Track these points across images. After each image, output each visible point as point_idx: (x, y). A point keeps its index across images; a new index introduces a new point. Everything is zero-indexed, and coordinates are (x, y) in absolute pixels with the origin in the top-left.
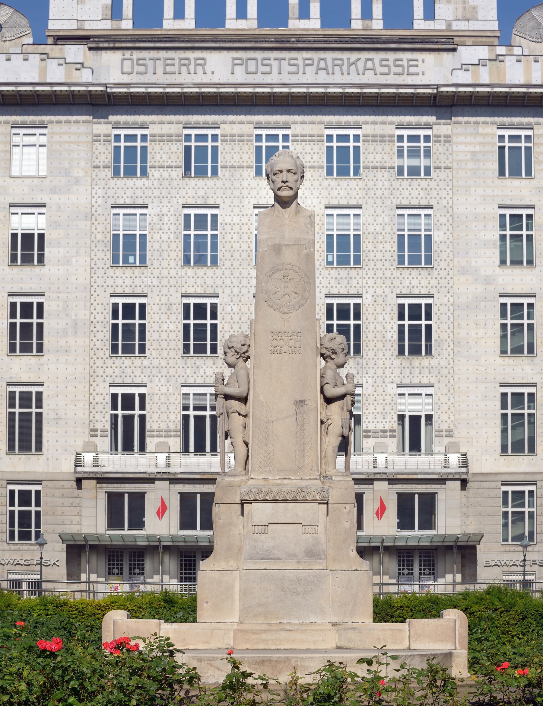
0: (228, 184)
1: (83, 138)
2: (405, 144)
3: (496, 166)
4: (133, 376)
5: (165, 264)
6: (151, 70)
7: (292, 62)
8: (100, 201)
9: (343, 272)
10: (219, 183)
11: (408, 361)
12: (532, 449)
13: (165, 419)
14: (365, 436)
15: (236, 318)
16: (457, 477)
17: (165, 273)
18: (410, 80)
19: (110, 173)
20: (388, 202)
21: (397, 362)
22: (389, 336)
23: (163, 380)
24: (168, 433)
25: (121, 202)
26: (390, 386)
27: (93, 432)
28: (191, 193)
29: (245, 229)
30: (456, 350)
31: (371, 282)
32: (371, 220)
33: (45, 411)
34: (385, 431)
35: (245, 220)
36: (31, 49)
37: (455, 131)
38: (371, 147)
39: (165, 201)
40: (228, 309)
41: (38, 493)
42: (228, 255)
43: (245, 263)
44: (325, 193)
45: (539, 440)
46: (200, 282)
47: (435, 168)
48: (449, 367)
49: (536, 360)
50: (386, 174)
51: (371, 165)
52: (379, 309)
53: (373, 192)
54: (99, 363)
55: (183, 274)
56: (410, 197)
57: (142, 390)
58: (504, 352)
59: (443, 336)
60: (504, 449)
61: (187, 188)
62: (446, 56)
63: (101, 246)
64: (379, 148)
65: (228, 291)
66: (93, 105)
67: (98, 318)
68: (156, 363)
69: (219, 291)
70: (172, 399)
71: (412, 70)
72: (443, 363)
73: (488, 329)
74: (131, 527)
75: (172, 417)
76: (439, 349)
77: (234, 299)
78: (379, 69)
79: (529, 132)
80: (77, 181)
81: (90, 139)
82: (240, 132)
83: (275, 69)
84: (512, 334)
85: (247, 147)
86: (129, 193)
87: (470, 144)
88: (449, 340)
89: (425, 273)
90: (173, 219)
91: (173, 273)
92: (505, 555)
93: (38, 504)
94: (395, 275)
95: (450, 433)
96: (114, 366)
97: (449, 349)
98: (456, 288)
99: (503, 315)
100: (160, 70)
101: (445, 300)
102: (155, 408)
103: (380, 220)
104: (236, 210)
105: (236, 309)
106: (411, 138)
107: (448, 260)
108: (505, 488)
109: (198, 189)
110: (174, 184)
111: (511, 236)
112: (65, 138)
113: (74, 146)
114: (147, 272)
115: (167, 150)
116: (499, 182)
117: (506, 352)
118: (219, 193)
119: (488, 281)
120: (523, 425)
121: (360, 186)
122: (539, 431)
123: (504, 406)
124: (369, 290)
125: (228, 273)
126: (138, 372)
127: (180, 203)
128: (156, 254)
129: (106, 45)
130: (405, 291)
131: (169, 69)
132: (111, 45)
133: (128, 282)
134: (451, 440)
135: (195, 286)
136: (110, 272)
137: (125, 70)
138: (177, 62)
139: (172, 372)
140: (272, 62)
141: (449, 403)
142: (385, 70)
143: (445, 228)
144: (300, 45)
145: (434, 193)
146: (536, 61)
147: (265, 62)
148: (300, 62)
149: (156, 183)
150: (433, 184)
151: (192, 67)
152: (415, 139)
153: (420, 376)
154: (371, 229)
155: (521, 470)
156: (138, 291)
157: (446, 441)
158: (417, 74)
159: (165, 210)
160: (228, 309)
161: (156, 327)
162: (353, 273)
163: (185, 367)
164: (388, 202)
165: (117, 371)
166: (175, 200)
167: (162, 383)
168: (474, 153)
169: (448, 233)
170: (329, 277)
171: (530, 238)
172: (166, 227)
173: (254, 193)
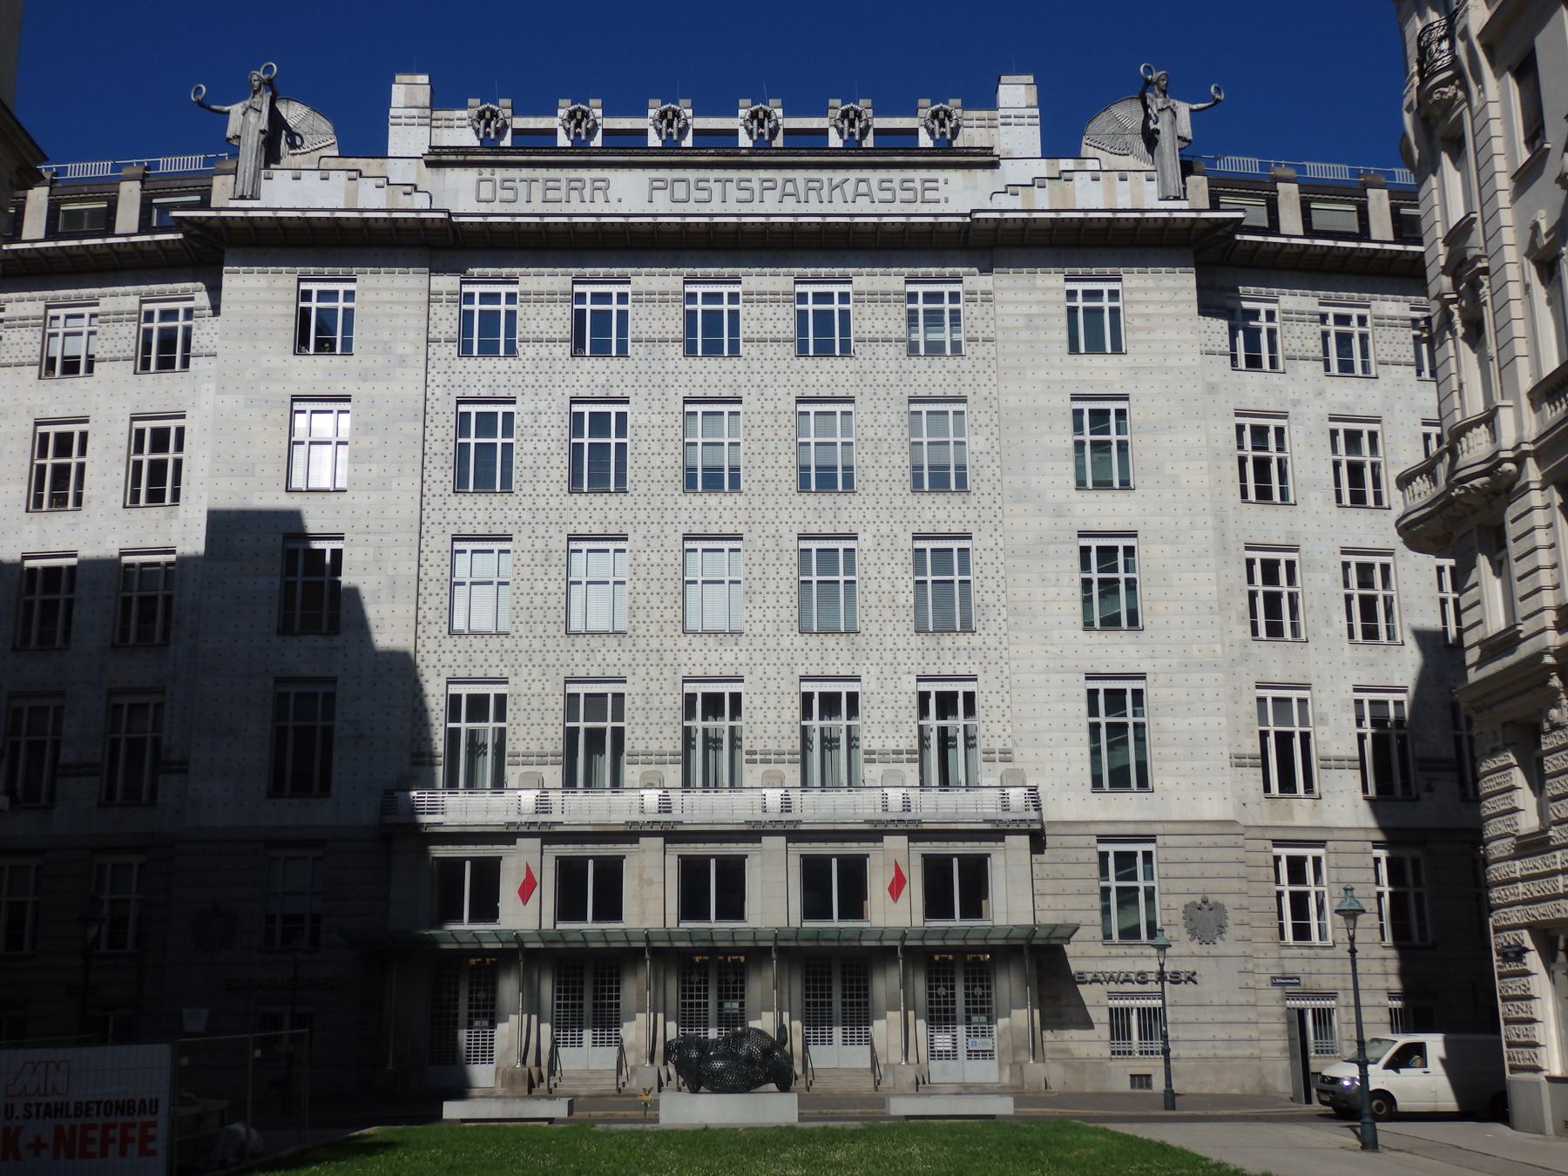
0: (643, 366)
1: (414, 297)
2: (921, 306)
3: (1064, 336)
4: (486, 665)
5: (541, 488)
6: (523, 196)
7: (743, 184)
10: (628, 364)
11: (934, 640)
12: (1143, 782)
13: (538, 734)
14: (867, 761)
15: (655, 572)
16: (1023, 826)
17: (541, 502)
18: (926, 209)
19: (453, 349)
20: (895, 393)
21: (916, 640)
22: (901, 599)
23: (536, 673)
24: (542, 758)
26: (906, 678)
28: (585, 380)
29: (670, 433)
30: (1011, 620)
31: (870, 515)
32: (868, 419)
34: (899, 752)
35: (669, 420)
36: (333, 163)
37: (998, 283)
38: (867, 310)
39: (543, 392)
42: (642, 475)
43: (669, 489)
44: (795, 379)
45: (1153, 767)
46: (597, 516)
47: (969, 340)
48: (1001, 647)
50: (892, 350)
51: (868, 336)
52: (885, 557)
53: (870, 377)
55: (571, 504)
56: (930, 384)
57: (500, 689)
58: (1088, 625)
59: (990, 599)
60: (1097, 782)
61: (578, 372)
62: (981, 175)
64: (879, 310)
65: (642, 530)
68: (524, 644)
69: (627, 530)
70: (550, 702)
71: (929, 195)
72: (991, 642)
73: (1061, 588)
74: (474, 918)
76: (983, 619)
77: (653, 542)
78: (878, 195)
80: (403, 361)
82: (662, 289)
83: (717, 196)
84: (1101, 595)
85: (673, 311)
86: (486, 379)
87: (1023, 302)
88: (999, 605)
89: (956, 499)
90: (555, 420)
91: (554, 502)
92: (1110, 962)
94: (909, 503)
95: (1006, 755)
96: (455, 651)
97: (1000, 619)
98: (1007, 522)
99: (1085, 566)
100: (537, 196)
101: (991, 543)
103: (883, 419)
104: (656, 405)
105: (655, 558)
106: (929, 297)
107: (994, 480)
109: (595, 375)
110: (558, 366)
111: (1093, 443)
113: (398, 309)
115: (547, 314)
117: (1092, 624)
118: (629, 379)
119: (1059, 512)
120: (1125, 742)
121: (851, 368)
123: (1093, 711)
124: (868, 527)
125: (642, 502)
126: (494, 659)
127: (568, 395)
128: (528, 474)
129: (452, 158)
130: (926, 529)
131: (551, 195)
132: (461, 158)
133: (482, 516)
134: (1009, 765)
135: (590, 522)
137: (482, 196)
138: (563, 184)
139: (551, 658)
140: (712, 184)
141: (1003, 706)
142: (888, 195)
143: (987, 431)
144: (754, 159)
145: (967, 379)
146: (1123, 179)
147: (701, 185)
148: (755, 185)
149: (529, 366)
150: (965, 364)
151: (587, 193)
152: (937, 297)
153: (954, 663)
154: (870, 433)
156: (498, 530)
157: (1001, 767)
158: (938, 202)
159: (542, 406)
160: (643, 558)
162: (842, 500)
163: (573, 650)
164: (895, 393)
165: (461, 658)
166: (559, 391)
167: (534, 675)
168: (1030, 317)
169: (992, 438)
170: (805, 508)
171: (1123, 446)
173: (684, 379)
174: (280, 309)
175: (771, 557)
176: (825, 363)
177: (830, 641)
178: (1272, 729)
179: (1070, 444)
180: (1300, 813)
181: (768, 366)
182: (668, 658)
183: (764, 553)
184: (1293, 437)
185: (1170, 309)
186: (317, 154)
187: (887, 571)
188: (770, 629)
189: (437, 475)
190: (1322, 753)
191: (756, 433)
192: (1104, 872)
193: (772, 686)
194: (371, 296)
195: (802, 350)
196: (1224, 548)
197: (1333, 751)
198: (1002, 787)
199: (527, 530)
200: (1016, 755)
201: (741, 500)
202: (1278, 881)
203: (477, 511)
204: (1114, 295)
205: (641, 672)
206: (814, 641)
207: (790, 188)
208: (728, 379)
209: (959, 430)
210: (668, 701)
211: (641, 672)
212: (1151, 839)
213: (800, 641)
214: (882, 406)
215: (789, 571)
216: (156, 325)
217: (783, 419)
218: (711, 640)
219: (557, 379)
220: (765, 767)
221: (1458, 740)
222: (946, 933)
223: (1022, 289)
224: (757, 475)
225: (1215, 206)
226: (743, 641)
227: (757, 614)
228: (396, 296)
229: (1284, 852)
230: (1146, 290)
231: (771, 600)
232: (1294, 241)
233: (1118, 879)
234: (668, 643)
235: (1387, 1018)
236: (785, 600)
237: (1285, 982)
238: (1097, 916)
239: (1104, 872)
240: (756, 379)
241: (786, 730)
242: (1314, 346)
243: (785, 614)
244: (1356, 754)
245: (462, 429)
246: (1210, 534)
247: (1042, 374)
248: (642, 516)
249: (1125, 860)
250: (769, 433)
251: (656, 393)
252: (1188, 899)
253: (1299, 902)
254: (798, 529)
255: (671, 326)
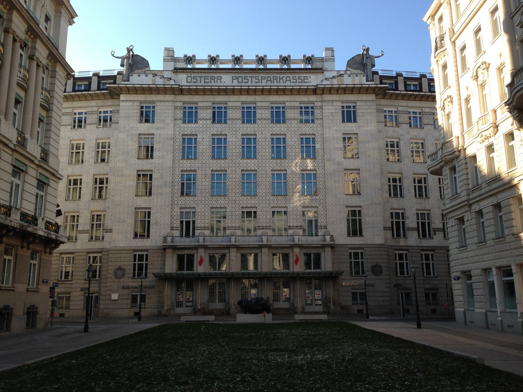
0: (231, 126)
1: (170, 108)
2: (303, 110)
3: (341, 118)
5: (204, 158)
6: (199, 81)
8: (177, 133)
9: (279, 161)
10: (227, 126)
12: (361, 234)
17: (204, 162)
18: (305, 84)
19: (181, 122)
20: (297, 133)
23: (203, 206)
24: (205, 228)
25: (186, 133)
27: (172, 228)
28: (215, 130)
29: (238, 144)
30: (327, 192)
32: (289, 140)
33: (152, 219)
35: (237, 140)
38: (289, 111)
39: (205, 133)
40: (231, 176)
41: (147, 255)
42: (230, 154)
43: (238, 158)
44: (270, 129)
46: (219, 165)
49: (361, 196)
54: (176, 199)
60: (349, 235)
63: (177, 151)
64: (293, 111)
65: (230, 169)
66: (175, 94)
67: (176, 180)
68: (200, 199)
69: (227, 169)
71: (306, 81)
72: (321, 198)
74: (187, 270)
75: (207, 221)
78: (292, 81)
79: (354, 105)
80: (168, 124)
81: (173, 108)
83: (250, 81)
86: (190, 129)
87: (330, 109)
90: (208, 140)
91: (207, 162)
93: (147, 260)
95: (325, 227)
98: (326, 167)
100: (203, 81)
101: (321, 172)
102: (199, 218)
103: (293, 140)
104: (234, 136)
105: (234, 176)
106: (305, 108)
108: (350, 251)
109: (218, 128)
110: (208, 126)
112: (163, 107)
113: (166, 111)
114: (197, 161)
116: (342, 124)
118: (227, 129)
119: (339, 164)
122: (363, 226)
125: (230, 161)
126: (192, 203)
128: (201, 154)
131: (206, 81)
133: (189, 165)
136: (181, 161)
139: (207, 202)
140: (248, 78)
142: (295, 81)
145: (315, 129)
146: (357, 76)
148: (260, 78)
150: (315, 125)
151: (216, 80)
152: (308, 108)
154: (290, 143)
155: (357, 243)
156: (193, 169)
157: (324, 230)
159: (204, 136)
160: (231, 176)
161: (200, 184)
162: (283, 161)
172: (205, 143)
173: (241, 129)
174: (135, 111)
175: (264, 176)
176: (278, 125)
177: (280, 198)
178: (394, 220)
179: (342, 146)
180: (402, 242)
181: (263, 126)
182: (237, 202)
183: (262, 174)
184: (402, 144)
185: (369, 111)
186: (144, 70)
187: (294, 179)
188: (264, 194)
189: (177, 155)
190: (407, 226)
191: (260, 143)
192: (351, 258)
193: (264, 209)
194: (159, 108)
195: (272, 122)
196: (382, 173)
197: (411, 226)
198: (324, 236)
199: (200, 169)
200: (328, 227)
201: (256, 161)
202: (396, 260)
203: (187, 164)
204: (354, 107)
205: (230, 206)
206: (275, 198)
207: (269, 79)
208: (253, 129)
209: (314, 142)
210: (237, 213)
211: (230, 206)
212: (363, 248)
213: (271, 198)
214: (293, 136)
215: (269, 179)
216: (102, 115)
217: (267, 140)
218: (248, 198)
219: (208, 129)
220: (262, 230)
221: (444, 223)
222: (309, 273)
223: (331, 105)
224: (260, 154)
225: (381, 83)
226: (257, 198)
227: (261, 191)
228: (166, 108)
229: (397, 252)
230: (363, 106)
231: (264, 187)
232: (402, 92)
233: (354, 259)
234: (237, 198)
235: (424, 295)
236: (268, 187)
237: (397, 286)
238: (349, 269)
239: (351, 258)
240: (260, 129)
241: (268, 221)
242: (407, 120)
243: (268, 191)
244: (416, 227)
245: (184, 143)
246: (379, 170)
247: (335, 128)
248: (230, 165)
249: (356, 254)
250: (264, 143)
251: (234, 133)
252: (372, 264)
253: (401, 265)
254: (271, 168)
255: (238, 115)
